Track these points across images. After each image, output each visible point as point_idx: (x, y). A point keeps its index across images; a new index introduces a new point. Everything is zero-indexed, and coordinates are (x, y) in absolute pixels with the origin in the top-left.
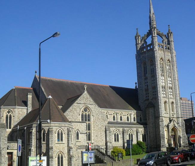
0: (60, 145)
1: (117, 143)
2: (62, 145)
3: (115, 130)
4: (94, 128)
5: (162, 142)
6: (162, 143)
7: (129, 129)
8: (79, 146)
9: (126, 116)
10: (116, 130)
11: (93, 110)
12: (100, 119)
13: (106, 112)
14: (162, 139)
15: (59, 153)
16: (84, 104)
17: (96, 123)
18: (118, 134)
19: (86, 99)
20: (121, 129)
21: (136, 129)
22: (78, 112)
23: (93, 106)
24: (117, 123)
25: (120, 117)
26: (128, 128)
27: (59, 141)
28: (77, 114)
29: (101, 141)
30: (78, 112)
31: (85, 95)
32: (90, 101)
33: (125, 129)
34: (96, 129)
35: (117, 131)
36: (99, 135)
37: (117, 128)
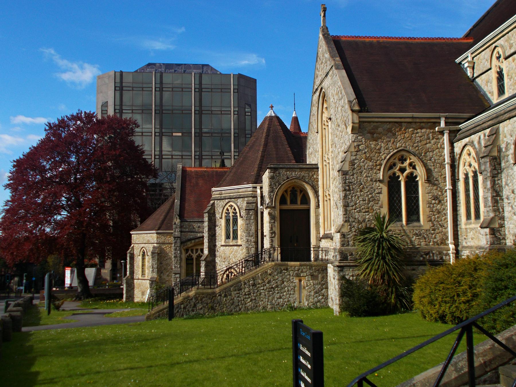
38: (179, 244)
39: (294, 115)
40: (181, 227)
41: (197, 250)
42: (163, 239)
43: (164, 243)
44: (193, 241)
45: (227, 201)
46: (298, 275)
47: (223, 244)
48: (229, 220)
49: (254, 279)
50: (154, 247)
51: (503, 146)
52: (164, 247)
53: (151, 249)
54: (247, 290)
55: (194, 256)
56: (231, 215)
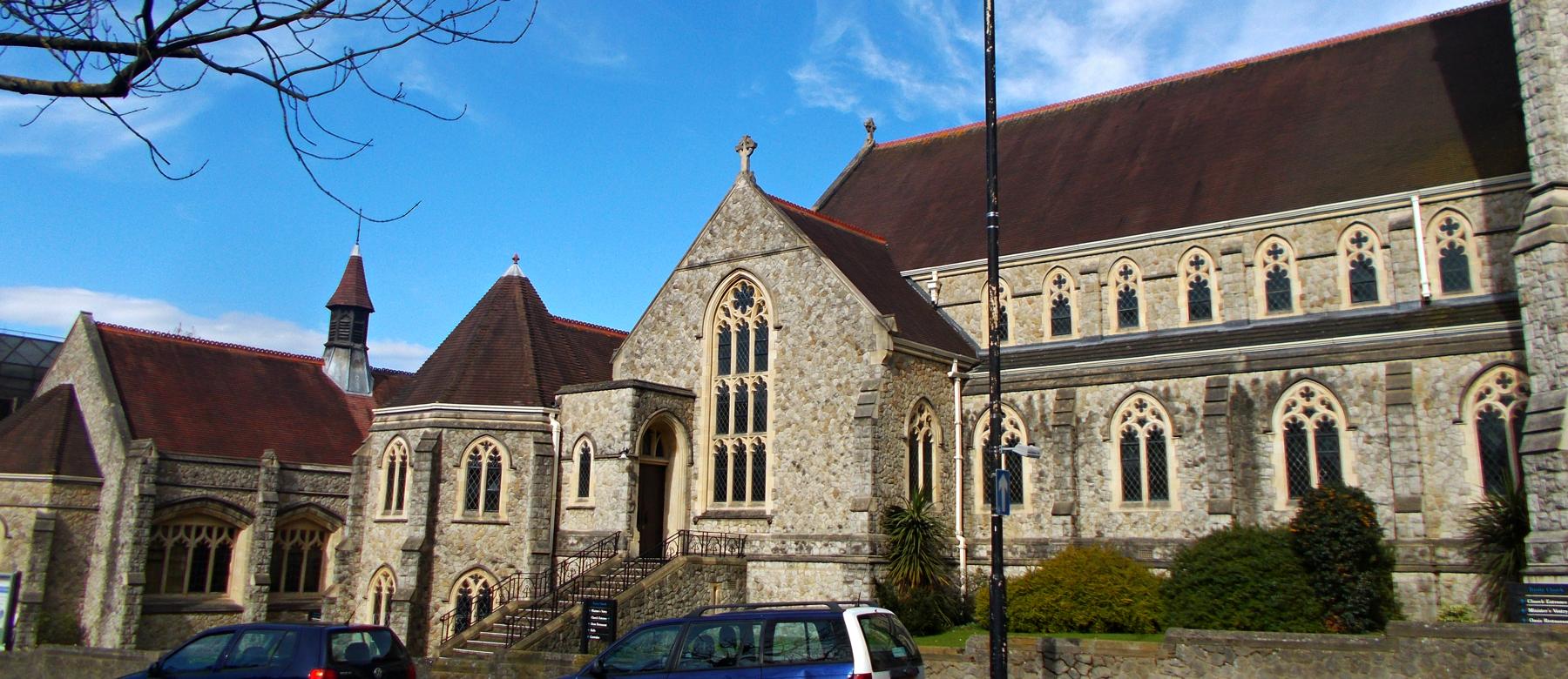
0: (388, 532)
1: (1145, 508)
2: (396, 528)
3: (1134, 399)
4: (785, 409)
5: (1533, 502)
6: (1534, 520)
7: (1288, 383)
8: (581, 539)
9: (1343, 265)
10: (1141, 406)
11: (781, 288)
12: (824, 344)
13: (1119, 267)
14: (1529, 463)
15: (379, 575)
16: (730, 259)
17: (801, 373)
18: (1156, 438)
19: (742, 228)
20: (1192, 390)
21: (1381, 368)
22: (693, 318)
23: (781, 262)
24: (1156, 343)
25: (1259, 277)
26: (1277, 376)
27: (724, 499)
28: (690, 335)
29: (829, 498)
30: (693, 318)
31: (739, 205)
32: (764, 231)
33: (1245, 379)
34: (797, 417)
35: (1146, 413)
36: (816, 459)
37: (1149, 385)
38: (149, 513)
39: (355, 253)
40: (158, 471)
41: (177, 528)
42: (67, 496)
43: (68, 508)
44: (178, 508)
45: (476, 432)
46: (713, 581)
47: (458, 517)
48: (479, 471)
49: (661, 585)
50: (40, 517)
51: (1084, 416)
52: (65, 516)
53: (33, 522)
54: (650, 605)
55: (169, 543)
56: (485, 461)
